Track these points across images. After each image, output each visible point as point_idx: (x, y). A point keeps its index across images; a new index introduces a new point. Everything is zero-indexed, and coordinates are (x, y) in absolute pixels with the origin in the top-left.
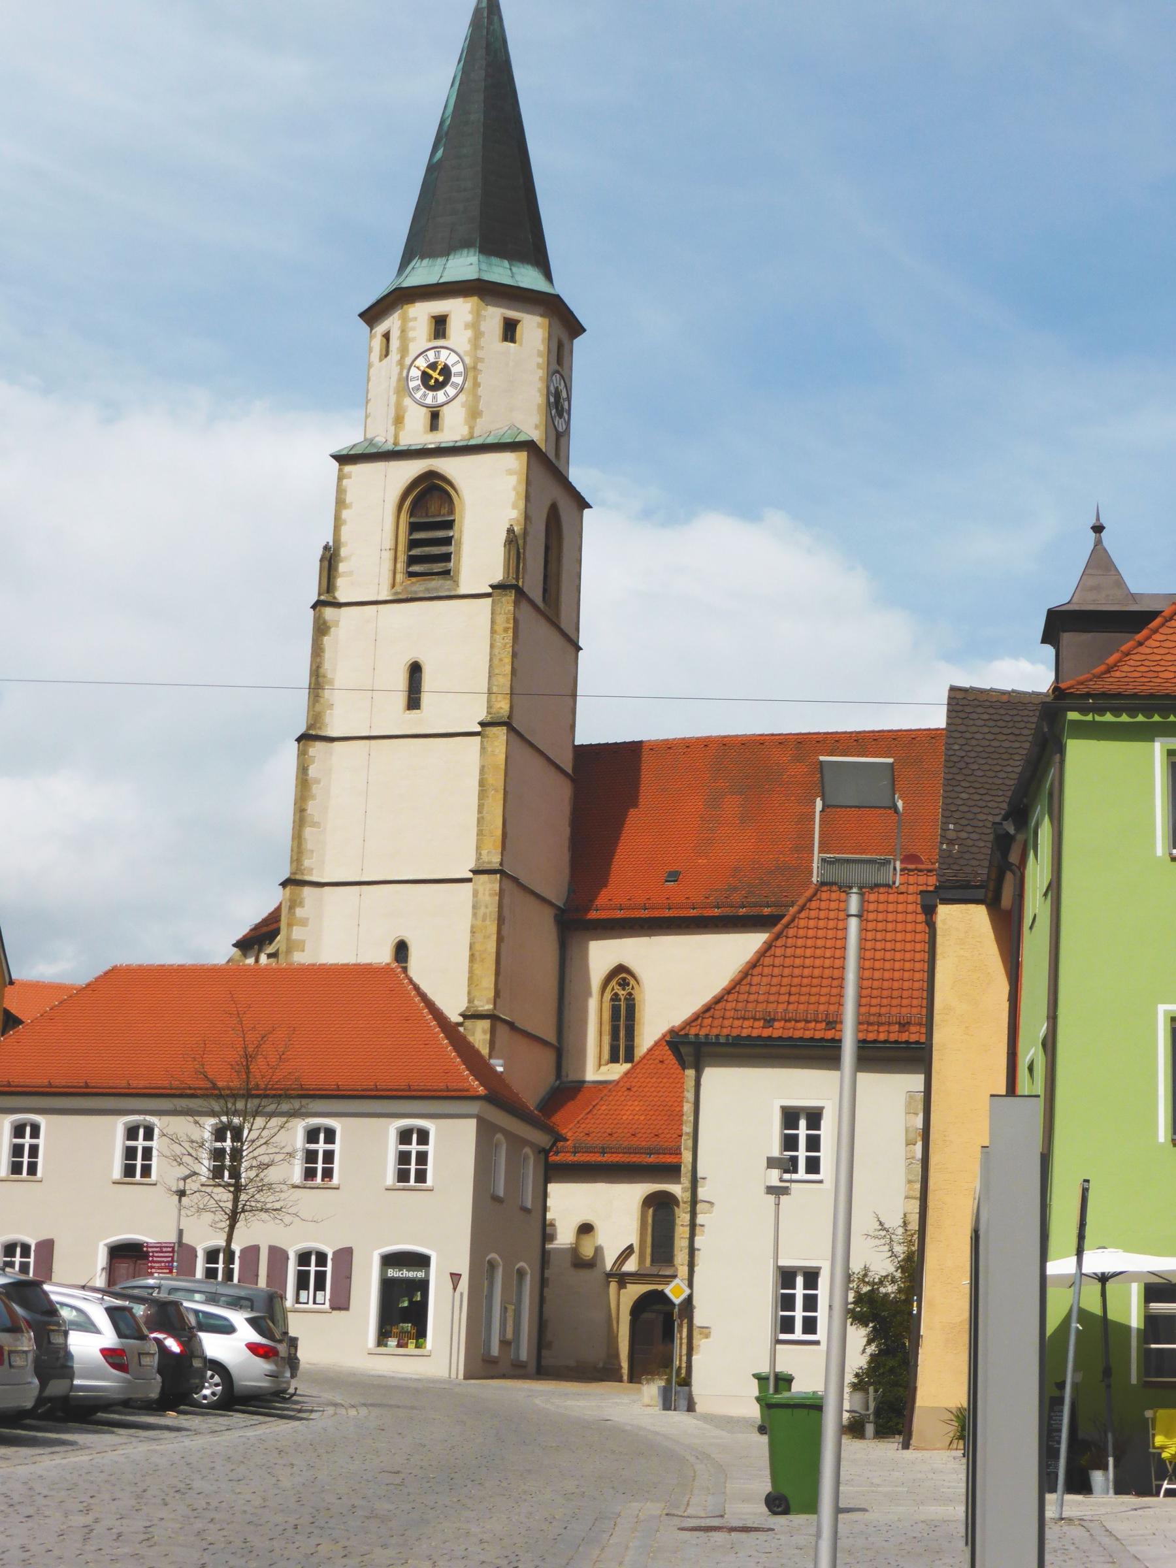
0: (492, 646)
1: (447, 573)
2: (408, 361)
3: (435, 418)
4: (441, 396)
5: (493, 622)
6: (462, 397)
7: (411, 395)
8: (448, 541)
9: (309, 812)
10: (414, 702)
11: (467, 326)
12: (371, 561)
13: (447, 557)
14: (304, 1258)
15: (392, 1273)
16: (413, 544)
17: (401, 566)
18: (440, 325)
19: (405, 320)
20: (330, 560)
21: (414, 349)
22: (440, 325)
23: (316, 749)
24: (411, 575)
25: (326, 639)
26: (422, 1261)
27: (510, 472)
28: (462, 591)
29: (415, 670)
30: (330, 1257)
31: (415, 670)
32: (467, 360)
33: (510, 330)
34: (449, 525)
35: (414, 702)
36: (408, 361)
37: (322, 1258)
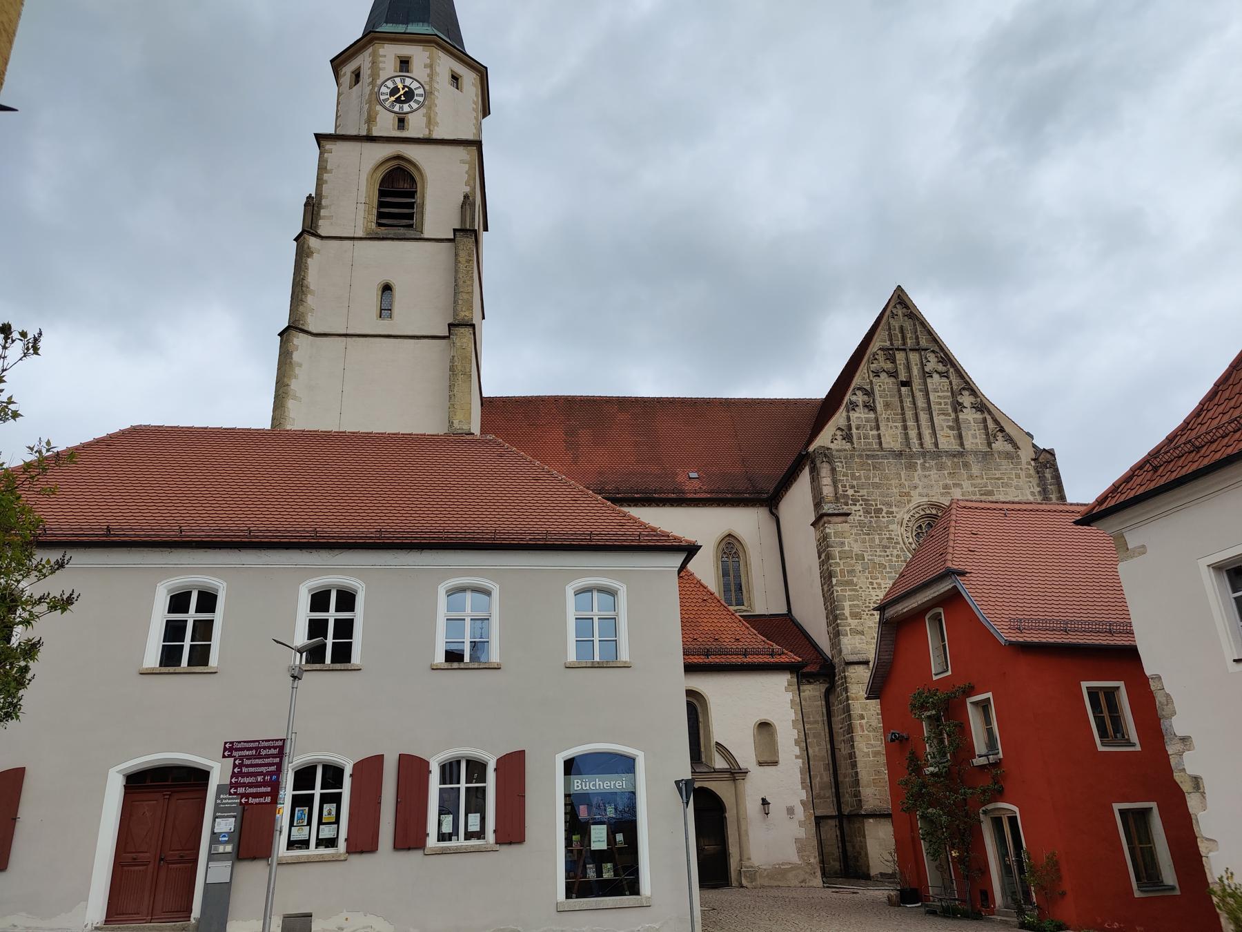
0: (456, 271)
1: (411, 226)
2: (379, 82)
3: (402, 122)
4: (406, 108)
5: (456, 255)
6: (423, 110)
7: (381, 105)
8: (411, 205)
9: (292, 387)
10: (385, 311)
11: (425, 66)
12: (352, 207)
13: (411, 216)
14: (449, 771)
15: (581, 784)
16: (381, 204)
17: (374, 218)
18: (405, 64)
19: (374, 55)
20: (313, 207)
21: (383, 75)
22: (405, 64)
23: (299, 340)
24: (379, 225)
25: (309, 260)
26: (626, 764)
27: (462, 162)
28: (426, 236)
29: (387, 288)
30: (348, 771)
31: (387, 288)
32: (427, 87)
33: (455, 78)
34: (412, 194)
35: (385, 311)
36: (379, 82)
37: (477, 769)
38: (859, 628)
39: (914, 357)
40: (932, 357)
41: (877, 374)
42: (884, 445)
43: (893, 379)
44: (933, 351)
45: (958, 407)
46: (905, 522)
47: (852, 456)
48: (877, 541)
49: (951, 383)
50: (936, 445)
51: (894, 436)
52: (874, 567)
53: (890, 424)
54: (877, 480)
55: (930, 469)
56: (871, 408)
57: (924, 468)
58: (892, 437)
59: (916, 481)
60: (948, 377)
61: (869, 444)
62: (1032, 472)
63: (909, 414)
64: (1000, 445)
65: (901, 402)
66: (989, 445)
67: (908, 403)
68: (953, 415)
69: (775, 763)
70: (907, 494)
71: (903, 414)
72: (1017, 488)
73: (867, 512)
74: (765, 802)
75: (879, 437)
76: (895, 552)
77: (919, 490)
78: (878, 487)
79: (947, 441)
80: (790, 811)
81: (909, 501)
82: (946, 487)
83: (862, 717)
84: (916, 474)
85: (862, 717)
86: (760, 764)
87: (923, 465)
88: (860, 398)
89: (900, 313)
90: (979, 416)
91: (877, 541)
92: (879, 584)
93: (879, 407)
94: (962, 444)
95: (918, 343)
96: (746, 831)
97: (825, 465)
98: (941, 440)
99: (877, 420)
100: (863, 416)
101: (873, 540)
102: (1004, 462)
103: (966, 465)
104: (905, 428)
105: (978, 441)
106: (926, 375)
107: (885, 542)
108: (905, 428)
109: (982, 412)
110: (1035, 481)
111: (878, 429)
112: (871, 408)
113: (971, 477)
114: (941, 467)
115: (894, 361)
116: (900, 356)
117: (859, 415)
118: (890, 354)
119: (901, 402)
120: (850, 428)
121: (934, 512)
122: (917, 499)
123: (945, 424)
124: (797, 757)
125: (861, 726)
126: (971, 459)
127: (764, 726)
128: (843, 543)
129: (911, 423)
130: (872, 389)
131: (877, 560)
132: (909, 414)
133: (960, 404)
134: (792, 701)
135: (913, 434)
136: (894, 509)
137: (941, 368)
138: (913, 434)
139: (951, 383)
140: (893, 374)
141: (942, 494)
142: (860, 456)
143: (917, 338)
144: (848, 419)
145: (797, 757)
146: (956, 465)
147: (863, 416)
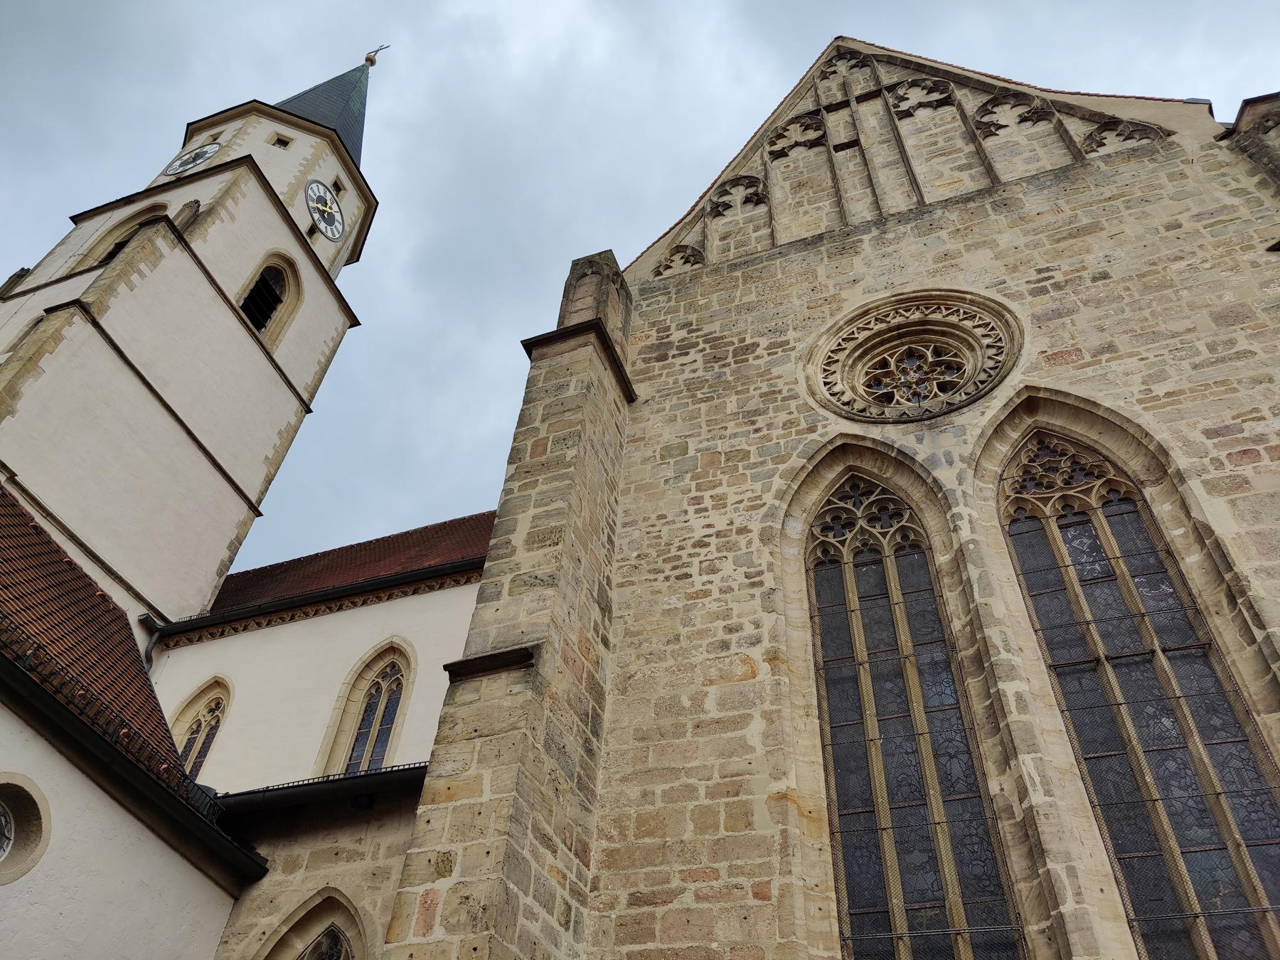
90: (1043, 127)
121: (917, 316)
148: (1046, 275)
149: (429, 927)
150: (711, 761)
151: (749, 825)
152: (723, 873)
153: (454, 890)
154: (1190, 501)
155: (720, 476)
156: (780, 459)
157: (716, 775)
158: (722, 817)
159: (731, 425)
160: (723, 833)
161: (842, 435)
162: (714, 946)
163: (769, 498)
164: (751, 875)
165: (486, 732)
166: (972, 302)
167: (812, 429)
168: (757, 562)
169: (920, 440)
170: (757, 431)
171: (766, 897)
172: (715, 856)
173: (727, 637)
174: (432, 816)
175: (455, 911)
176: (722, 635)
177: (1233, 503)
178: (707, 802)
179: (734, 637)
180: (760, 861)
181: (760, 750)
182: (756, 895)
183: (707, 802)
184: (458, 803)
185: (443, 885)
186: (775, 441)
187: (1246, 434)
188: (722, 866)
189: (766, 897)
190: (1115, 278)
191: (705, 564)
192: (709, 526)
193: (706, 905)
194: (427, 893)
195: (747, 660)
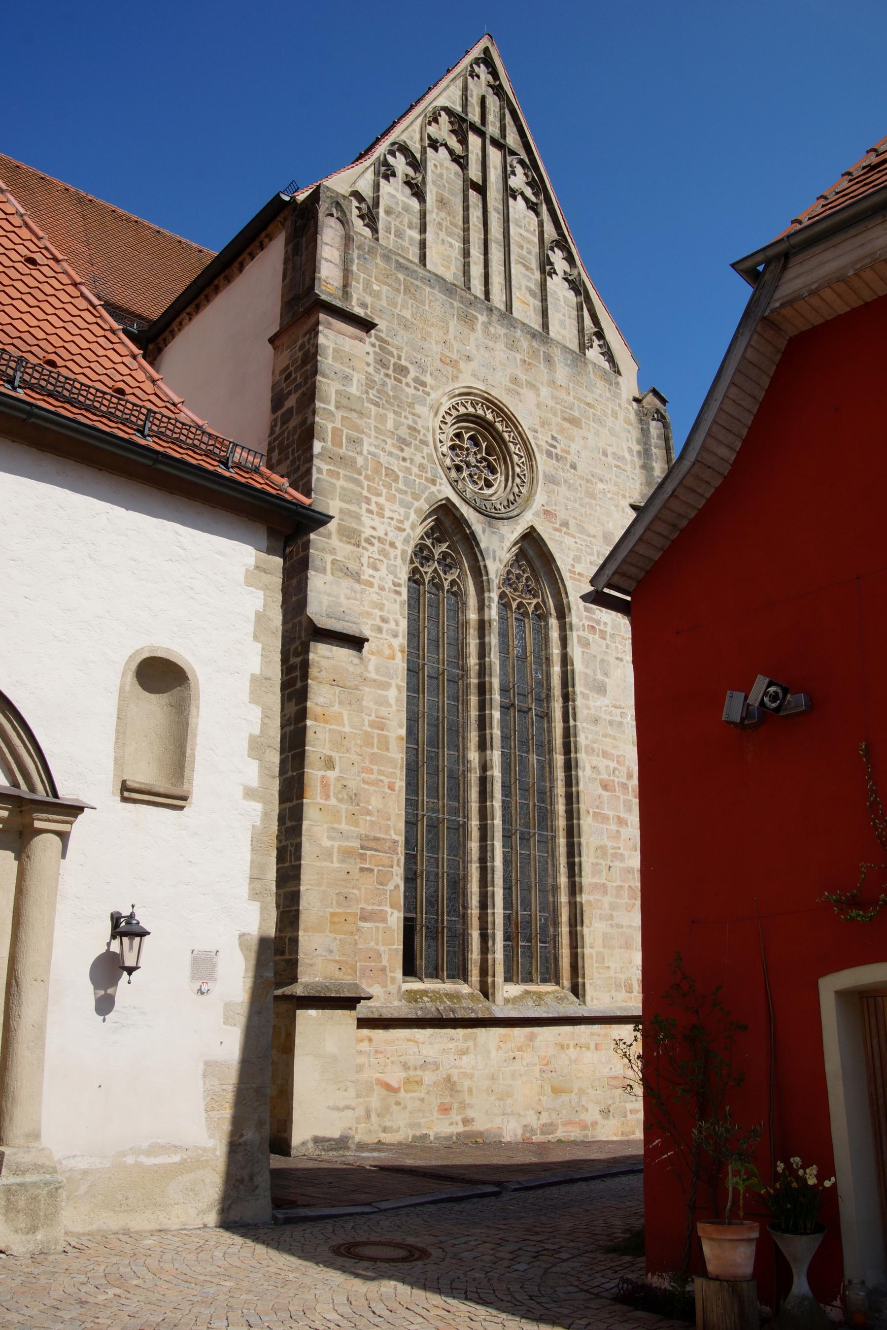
38: (353, 566)
39: (495, 156)
40: (519, 170)
41: (434, 144)
42: (429, 266)
43: (455, 167)
44: (521, 162)
45: (546, 268)
46: (442, 412)
47: (372, 251)
48: (390, 424)
49: (541, 224)
50: (509, 306)
51: (446, 259)
52: (377, 471)
53: (442, 235)
54: (407, 314)
55: (495, 338)
56: (418, 192)
57: (486, 332)
58: (444, 257)
59: (471, 348)
60: (537, 214)
61: (402, 248)
62: (632, 417)
63: (476, 236)
64: (594, 354)
65: (466, 208)
66: (583, 347)
67: (476, 215)
68: (537, 275)
69: (175, 800)
70: (453, 363)
71: (466, 230)
72: (612, 432)
73: (382, 363)
74: (125, 928)
75: (423, 245)
76: (418, 459)
77: (474, 365)
78: (406, 327)
79: (526, 309)
80: (203, 966)
81: (455, 378)
82: (515, 380)
83: (329, 764)
84: (473, 336)
85: (329, 764)
86: (128, 792)
87: (487, 325)
88: (399, 163)
89: (482, 76)
91: (390, 424)
92: (381, 507)
93: (430, 198)
94: (545, 326)
95: (504, 136)
96: (40, 1028)
97: (332, 222)
98: (516, 304)
99: (423, 215)
100: (400, 196)
101: (382, 419)
102: (600, 384)
103: (549, 360)
104: (466, 254)
105: (565, 332)
106: (510, 193)
107: (403, 432)
108: (466, 254)
109: (577, 293)
110: (635, 433)
111: (423, 230)
112: (418, 192)
113: (552, 383)
114: (512, 345)
115: (464, 141)
116: (474, 140)
117: (394, 193)
118: (461, 126)
119: (466, 208)
120: (376, 204)
121: (490, 417)
122: (466, 381)
123: (524, 283)
124: (249, 794)
125: (325, 785)
126: (557, 354)
127: (160, 675)
128: (347, 378)
129: (476, 253)
130: (424, 160)
131: (384, 459)
132: (476, 236)
133: (551, 264)
134: (260, 618)
135: (476, 271)
136: (428, 379)
137: (528, 192)
138: (476, 271)
139: (541, 224)
140: (461, 161)
141: (509, 391)
142: (387, 258)
143: (503, 129)
144: (377, 187)
145: (249, 794)
146: (535, 352)
147: (400, 196)
148: (555, 443)
149: (327, 797)
150: (371, 705)
151: (387, 749)
152: (375, 771)
153: (338, 779)
154: (569, 642)
155: (382, 488)
156: (416, 497)
157: (373, 715)
158: (376, 740)
159: (389, 441)
160: (375, 750)
161: (447, 499)
162: (370, 808)
163: (407, 525)
164: (387, 777)
165: (341, 684)
166: (519, 433)
167: (434, 482)
168: (399, 576)
169: (484, 531)
170: (404, 459)
171: (393, 790)
172: (372, 761)
173: (381, 624)
174: (317, 730)
175: (340, 792)
176: (378, 622)
177: (583, 652)
178: (369, 729)
179: (385, 626)
180: (391, 770)
181: (394, 708)
182: (389, 788)
183: (369, 729)
184: (332, 727)
185: (332, 775)
186: (413, 477)
187: (594, 616)
188: (375, 768)
189: (393, 790)
190: (578, 473)
191: (372, 560)
192: (374, 528)
193: (366, 786)
194: (323, 777)
195: (391, 646)
